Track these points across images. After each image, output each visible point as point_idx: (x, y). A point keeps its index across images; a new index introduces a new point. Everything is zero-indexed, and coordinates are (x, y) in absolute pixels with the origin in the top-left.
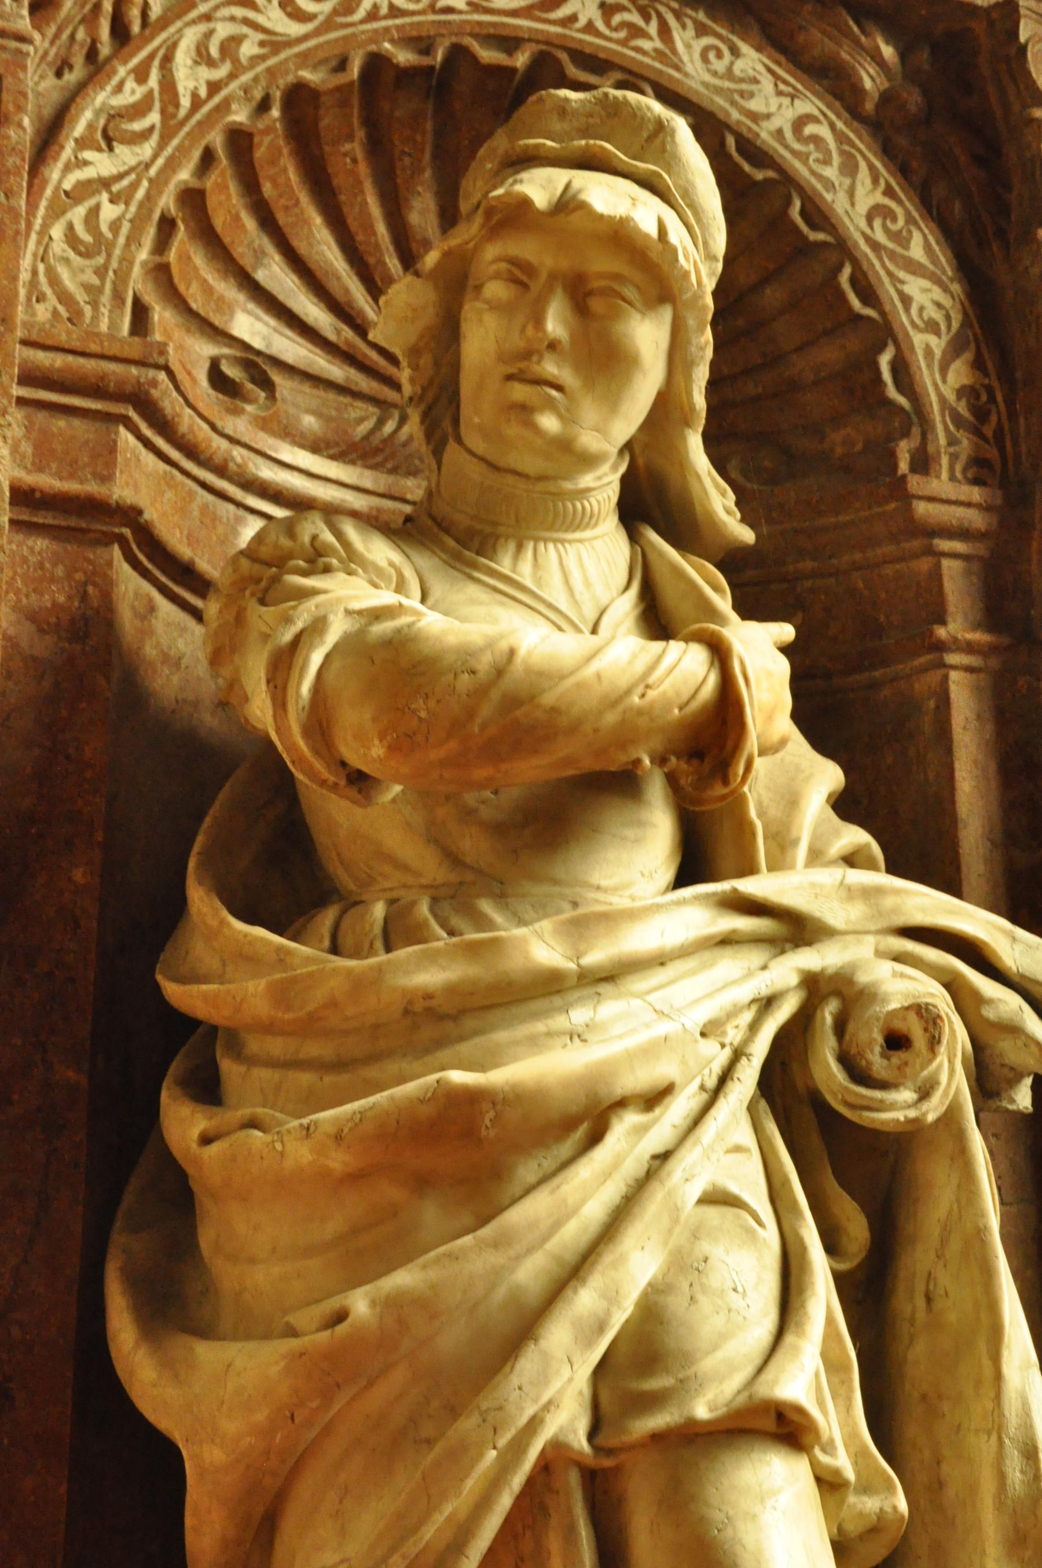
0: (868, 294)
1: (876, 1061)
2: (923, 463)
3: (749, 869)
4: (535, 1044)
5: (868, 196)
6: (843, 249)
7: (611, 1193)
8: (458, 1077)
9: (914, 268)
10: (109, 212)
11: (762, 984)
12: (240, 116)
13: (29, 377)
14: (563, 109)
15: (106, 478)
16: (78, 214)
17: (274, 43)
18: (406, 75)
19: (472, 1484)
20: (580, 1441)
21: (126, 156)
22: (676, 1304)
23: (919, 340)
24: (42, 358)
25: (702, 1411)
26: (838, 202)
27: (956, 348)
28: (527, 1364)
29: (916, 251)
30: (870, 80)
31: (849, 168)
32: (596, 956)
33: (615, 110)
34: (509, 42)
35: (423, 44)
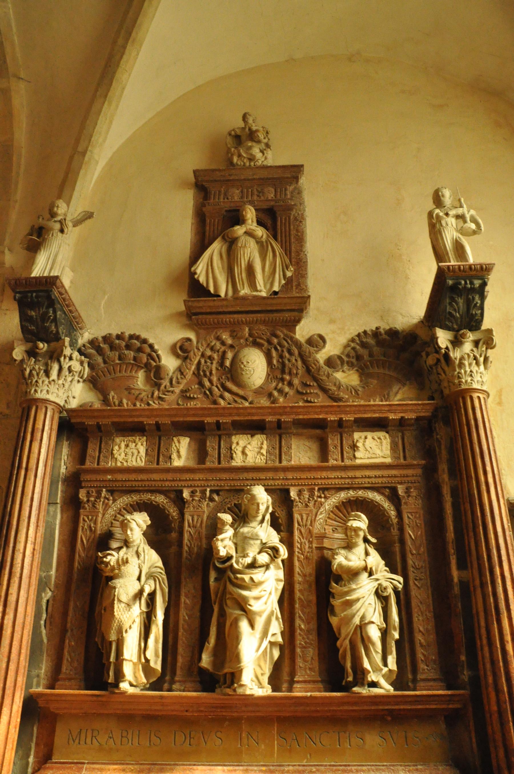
0: (388, 513)
1: (383, 591)
2: (394, 529)
3: (374, 575)
4: (354, 594)
5: (387, 504)
6: (385, 510)
7: (361, 604)
8: (348, 598)
9: (392, 510)
10: (321, 520)
11: (374, 585)
12: (331, 509)
13: (316, 537)
14: (352, 515)
15: (323, 544)
16: (319, 522)
17: (334, 502)
18: (346, 502)
19: (351, 628)
20: (359, 624)
21: (322, 515)
22: (366, 613)
23: (393, 517)
24: (318, 535)
25: (366, 622)
26: (384, 506)
27: (396, 518)
28: (354, 619)
29: (392, 509)
30: (387, 494)
31: (385, 502)
32: (358, 586)
33: (356, 514)
34: (354, 497)
35: (346, 499)
